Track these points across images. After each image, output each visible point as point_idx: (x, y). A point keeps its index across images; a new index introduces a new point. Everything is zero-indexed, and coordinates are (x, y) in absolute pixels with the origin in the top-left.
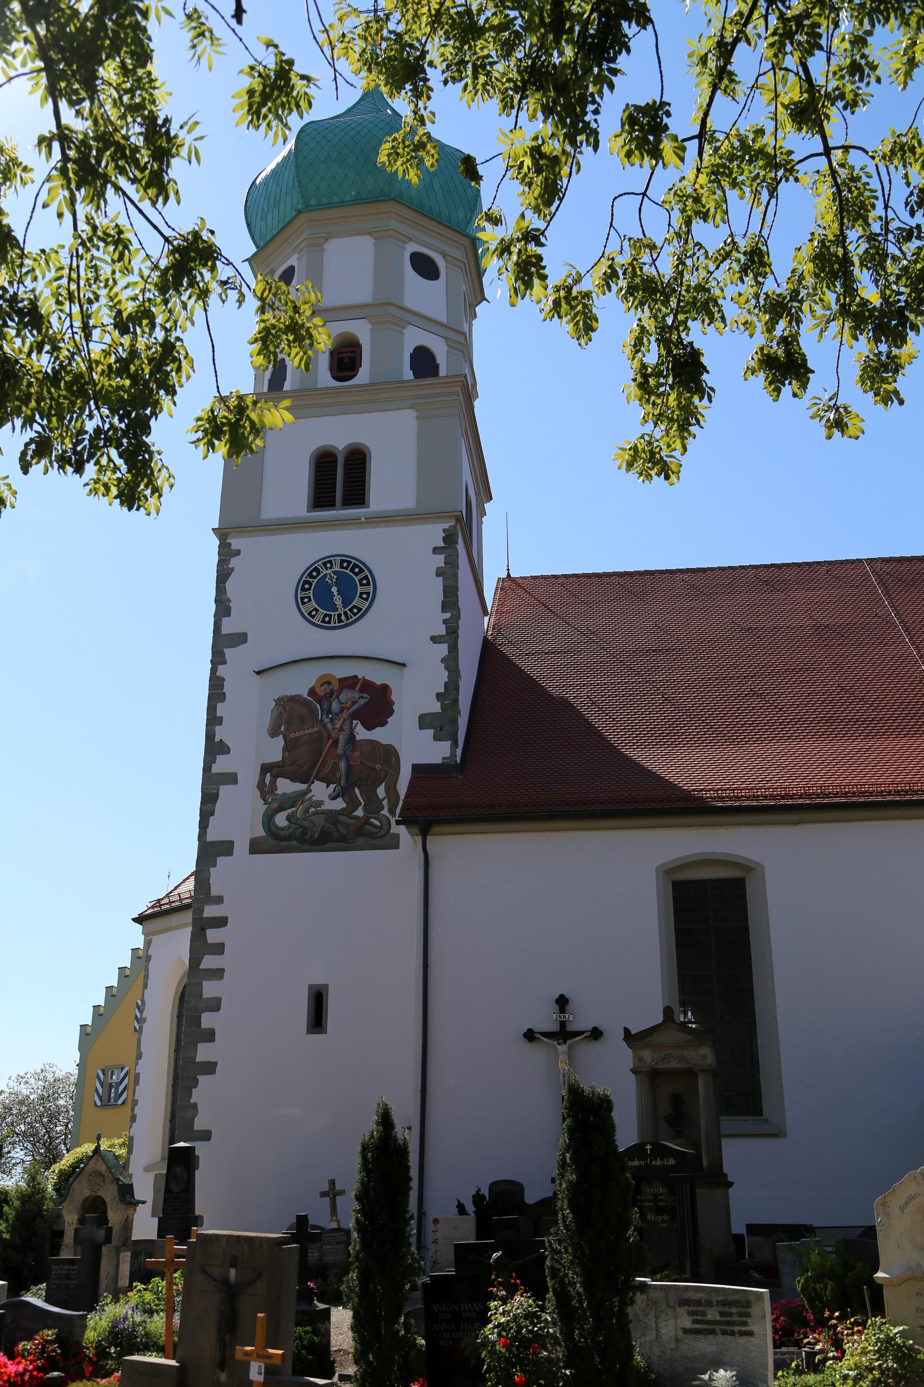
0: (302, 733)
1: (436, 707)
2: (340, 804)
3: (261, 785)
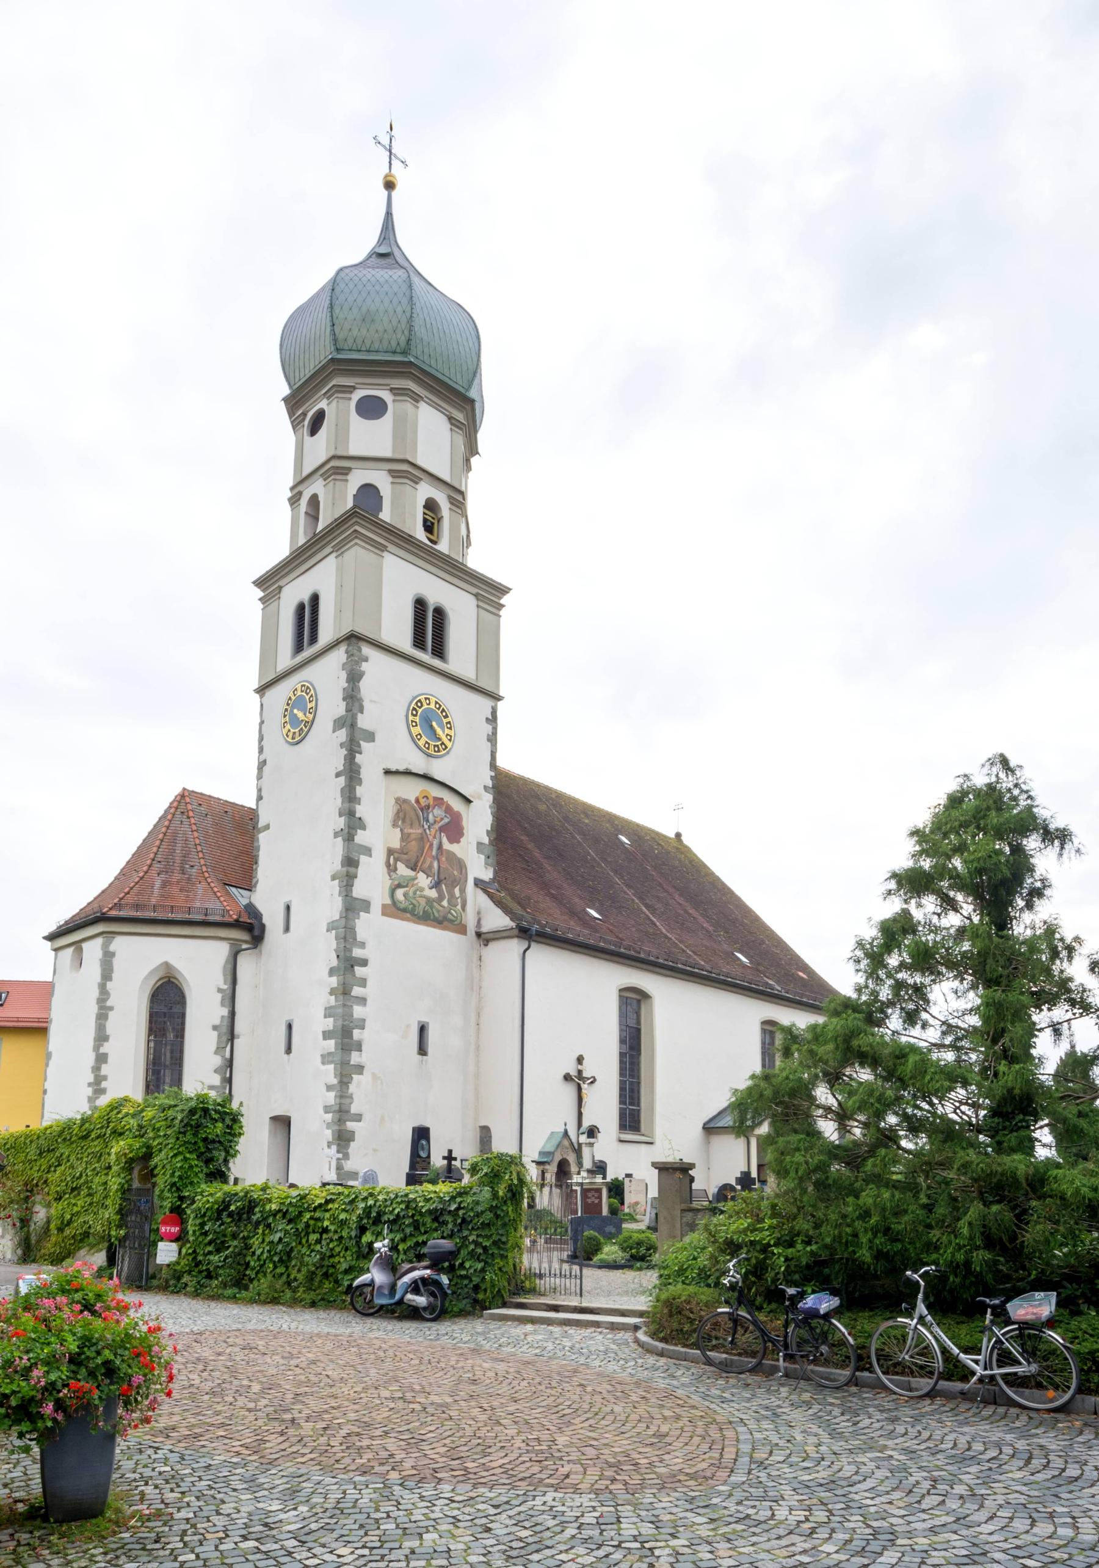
2: (433, 894)
3: (388, 865)
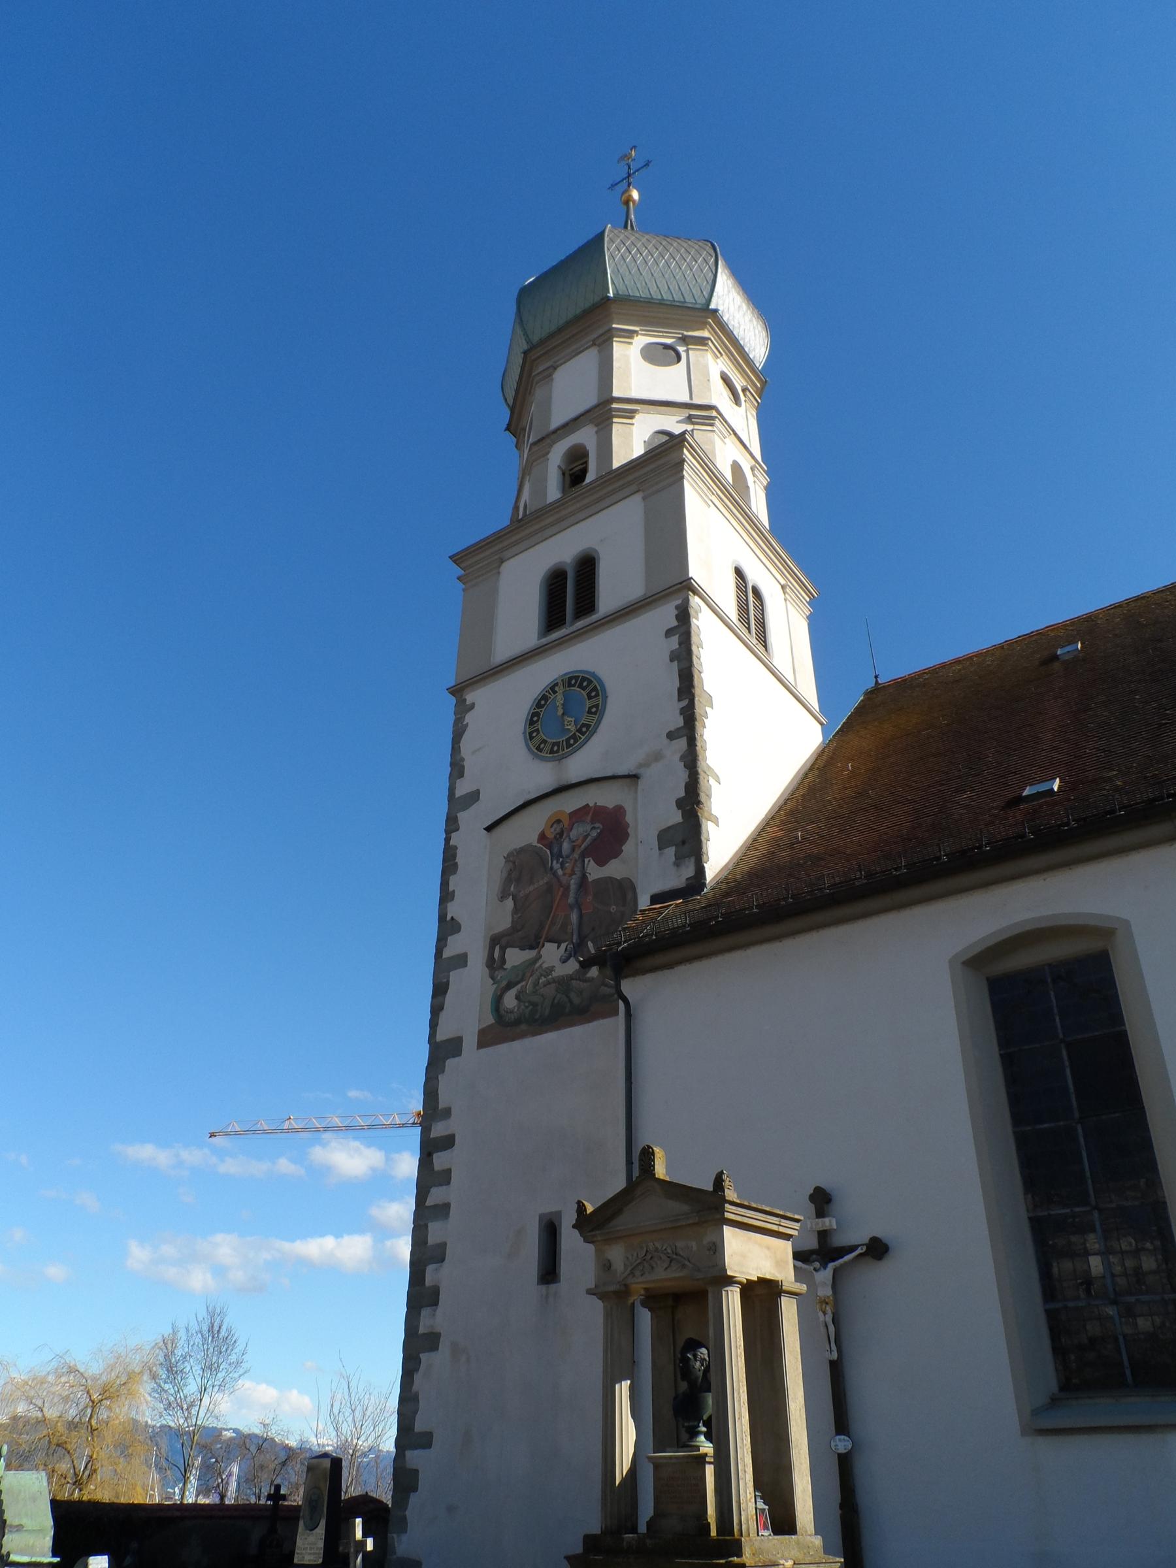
0: (531, 888)
1: (677, 817)
